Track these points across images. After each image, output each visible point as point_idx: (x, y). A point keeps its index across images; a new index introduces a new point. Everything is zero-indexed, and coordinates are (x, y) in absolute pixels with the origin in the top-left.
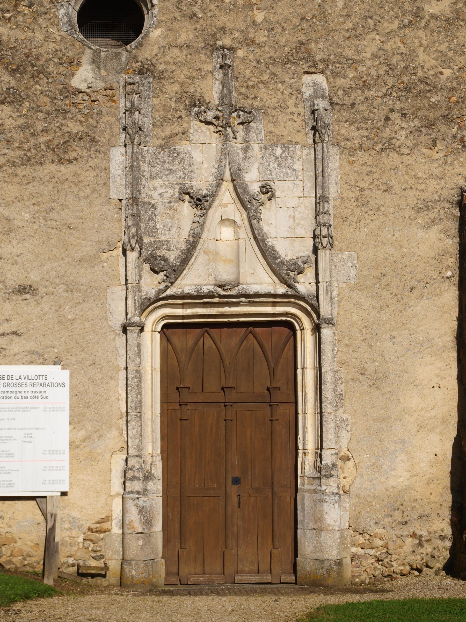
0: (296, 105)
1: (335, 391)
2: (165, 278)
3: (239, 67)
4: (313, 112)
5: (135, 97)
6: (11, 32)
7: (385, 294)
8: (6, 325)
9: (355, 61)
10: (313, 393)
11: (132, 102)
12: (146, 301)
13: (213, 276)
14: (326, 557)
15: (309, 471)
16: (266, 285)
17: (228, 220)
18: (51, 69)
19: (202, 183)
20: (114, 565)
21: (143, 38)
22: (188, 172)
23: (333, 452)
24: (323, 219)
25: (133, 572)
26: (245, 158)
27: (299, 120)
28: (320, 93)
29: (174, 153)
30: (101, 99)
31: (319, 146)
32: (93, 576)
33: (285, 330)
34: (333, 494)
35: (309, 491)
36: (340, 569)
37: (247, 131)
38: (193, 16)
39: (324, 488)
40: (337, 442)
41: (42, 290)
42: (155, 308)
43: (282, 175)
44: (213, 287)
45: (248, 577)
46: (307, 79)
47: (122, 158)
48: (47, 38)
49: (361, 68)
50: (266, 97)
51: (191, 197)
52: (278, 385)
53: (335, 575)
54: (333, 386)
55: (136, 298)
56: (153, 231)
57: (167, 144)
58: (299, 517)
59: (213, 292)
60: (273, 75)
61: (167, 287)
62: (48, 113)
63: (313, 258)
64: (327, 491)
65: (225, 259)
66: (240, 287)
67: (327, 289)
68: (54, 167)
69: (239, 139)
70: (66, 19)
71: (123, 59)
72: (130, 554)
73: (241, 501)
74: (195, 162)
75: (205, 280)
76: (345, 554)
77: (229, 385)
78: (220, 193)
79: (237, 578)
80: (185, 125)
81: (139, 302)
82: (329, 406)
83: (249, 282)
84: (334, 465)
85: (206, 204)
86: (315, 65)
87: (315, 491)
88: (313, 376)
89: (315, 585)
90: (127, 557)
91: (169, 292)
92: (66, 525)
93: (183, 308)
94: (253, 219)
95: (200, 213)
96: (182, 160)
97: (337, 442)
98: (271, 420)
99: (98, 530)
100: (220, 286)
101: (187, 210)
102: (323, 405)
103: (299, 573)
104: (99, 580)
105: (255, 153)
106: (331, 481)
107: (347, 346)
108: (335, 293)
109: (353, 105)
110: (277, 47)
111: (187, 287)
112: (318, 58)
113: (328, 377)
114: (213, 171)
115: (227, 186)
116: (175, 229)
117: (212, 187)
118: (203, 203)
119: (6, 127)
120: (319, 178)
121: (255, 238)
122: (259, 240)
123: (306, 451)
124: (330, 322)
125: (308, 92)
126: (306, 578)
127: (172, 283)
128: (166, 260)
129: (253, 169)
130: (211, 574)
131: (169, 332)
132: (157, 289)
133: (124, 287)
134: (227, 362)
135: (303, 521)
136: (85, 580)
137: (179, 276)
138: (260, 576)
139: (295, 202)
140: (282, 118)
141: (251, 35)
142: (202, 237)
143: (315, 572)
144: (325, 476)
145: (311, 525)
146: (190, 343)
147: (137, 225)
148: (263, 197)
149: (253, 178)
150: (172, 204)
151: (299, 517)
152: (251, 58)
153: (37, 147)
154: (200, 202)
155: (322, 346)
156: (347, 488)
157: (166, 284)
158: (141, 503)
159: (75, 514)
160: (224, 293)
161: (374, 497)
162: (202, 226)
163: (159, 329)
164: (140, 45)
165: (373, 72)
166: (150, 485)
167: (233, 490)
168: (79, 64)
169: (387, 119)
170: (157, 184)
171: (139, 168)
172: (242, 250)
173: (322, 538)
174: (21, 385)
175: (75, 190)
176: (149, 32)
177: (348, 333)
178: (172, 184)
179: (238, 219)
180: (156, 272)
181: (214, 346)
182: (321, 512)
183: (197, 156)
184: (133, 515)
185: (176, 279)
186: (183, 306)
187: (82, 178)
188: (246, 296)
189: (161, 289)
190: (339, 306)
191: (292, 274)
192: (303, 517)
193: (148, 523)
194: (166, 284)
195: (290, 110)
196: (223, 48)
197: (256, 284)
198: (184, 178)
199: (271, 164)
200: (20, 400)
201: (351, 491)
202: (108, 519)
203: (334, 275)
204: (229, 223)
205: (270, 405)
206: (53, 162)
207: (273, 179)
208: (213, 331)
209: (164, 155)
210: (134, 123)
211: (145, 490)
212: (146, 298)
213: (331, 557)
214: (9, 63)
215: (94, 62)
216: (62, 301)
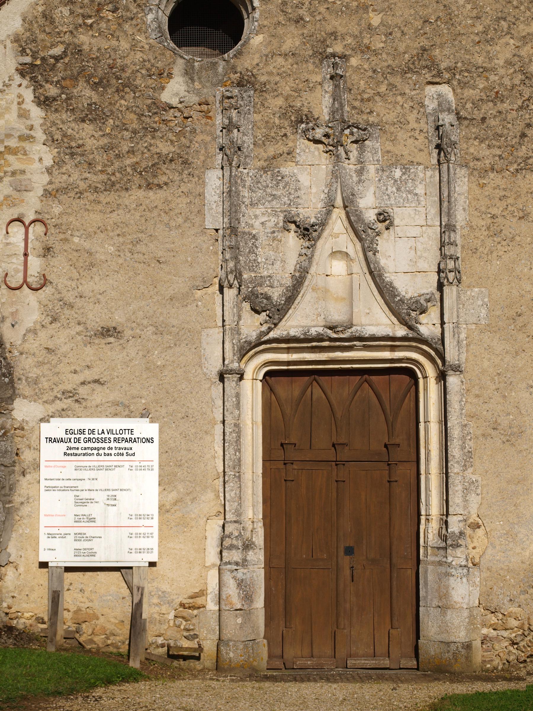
0: (418, 120)
1: (463, 448)
2: (268, 318)
3: (353, 78)
4: (437, 128)
5: (234, 113)
6: (93, 41)
7: (521, 336)
8: (87, 372)
9: (485, 70)
10: (438, 451)
11: (230, 119)
12: (246, 345)
13: (323, 317)
14: (452, 639)
15: (433, 540)
16: (383, 327)
17: (340, 252)
18: (138, 82)
19: (309, 210)
20: (209, 646)
21: (243, 45)
22: (294, 198)
23: (461, 518)
24: (449, 250)
25: (231, 654)
26: (360, 181)
27: (421, 138)
28: (445, 106)
29: (277, 176)
30: (195, 115)
31: (445, 167)
32: (185, 658)
33: (406, 379)
34: (461, 566)
35: (433, 563)
36: (468, 653)
37: (362, 151)
38: (299, 20)
39: (450, 559)
40: (465, 507)
41: (128, 333)
43: (402, 201)
44: (322, 328)
45: (363, 662)
46: (431, 90)
47: (219, 183)
48: (133, 47)
49: (492, 78)
50: (383, 112)
51: (298, 226)
52: (397, 441)
53: (463, 660)
54: (460, 443)
55: (234, 341)
56: (254, 266)
57: (270, 166)
58: (422, 593)
59: (322, 335)
60: (392, 86)
61: (270, 329)
62: (135, 132)
63: (437, 295)
64: (454, 563)
65: (336, 296)
66: (354, 329)
67: (454, 332)
68: (141, 193)
69: (353, 160)
70: (155, 25)
71: (220, 69)
72: (228, 634)
73: (355, 574)
74: (302, 186)
75: (313, 320)
76: (474, 636)
77: (341, 441)
78: (330, 222)
79: (350, 662)
80: (291, 144)
81: (237, 346)
82: (456, 465)
83: (363, 323)
84: (461, 533)
85: (315, 234)
86: (439, 74)
87: (440, 563)
88: (438, 430)
89: (440, 671)
90: (224, 638)
91: (272, 335)
92: (155, 600)
93: (288, 353)
94: (369, 251)
95: (307, 244)
96: (287, 184)
97: (465, 507)
98: (389, 482)
99: (191, 605)
100: (330, 328)
101: (292, 241)
102: (449, 464)
103: (421, 657)
104: (192, 663)
105: (370, 175)
106: (459, 552)
107: (477, 396)
108: (463, 336)
109: (484, 119)
110: (396, 54)
111: (292, 329)
112: (443, 66)
113: (455, 432)
114: (323, 196)
115: (338, 214)
116: (279, 262)
117: (321, 215)
118: (311, 233)
119: (87, 148)
120: (445, 203)
121: (371, 273)
122: (375, 274)
123: (430, 518)
124: (457, 369)
125: (431, 105)
126: (429, 663)
127: (276, 325)
128: (268, 298)
129: (368, 194)
130: (320, 657)
131: (272, 380)
132: (258, 332)
133: (221, 330)
134: (339, 415)
135: (425, 598)
136: (176, 663)
137: (284, 317)
138: (376, 660)
139: (415, 231)
140: (401, 135)
141: (366, 41)
142: (309, 272)
143: (440, 657)
144: (451, 545)
145: (435, 603)
146: (297, 393)
147: (236, 258)
148: (380, 226)
149: (368, 204)
150: (275, 235)
151: (421, 592)
152: (366, 66)
153: (122, 170)
154: (308, 232)
155: (448, 397)
156: (477, 560)
157: (268, 325)
158: (240, 575)
159: (165, 587)
160: (335, 336)
161: (508, 571)
162: (310, 259)
163: (261, 377)
164: (239, 53)
165: (507, 82)
166: (251, 555)
167: (346, 561)
168: (170, 76)
169: (523, 135)
170: (258, 212)
171: (238, 193)
172: (356, 286)
173: (448, 617)
174: (104, 440)
175: (165, 218)
176: (249, 39)
177: (477, 381)
178: (276, 211)
179: (351, 251)
180: (258, 312)
181: (324, 396)
182: (447, 587)
183: (304, 179)
184: (231, 589)
185: (281, 320)
186: (288, 350)
187: (173, 205)
188: (361, 339)
189: (263, 332)
190: (467, 351)
191: (413, 314)
192: (426, 592)
193: (248, 598)
194: (268, 325)
195: (411, 126)
196: (334, 55)
197: (372, 325)
198: (290, 204)
199: (389, 188)
200: (102, 458)
201: (482, 563)
202: (202, 593)
203: (462, 315)
204: (340, 255)
205: (388, 465)
206: (140, 187)
207: (391, 205)
208: (323, 380)
209: (266, 179)
210: (232, 142)
211: (245, 560)
213: (458, 640)
214: (91, 76)
215: (186, 73)
216: (150, 345)
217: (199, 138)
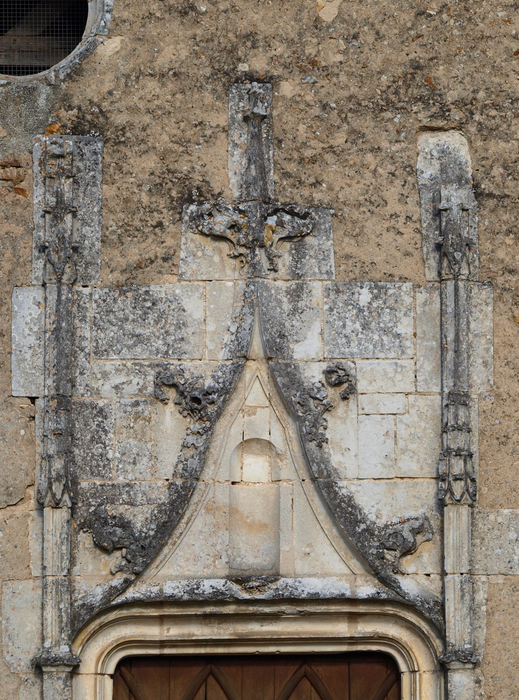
2: (124, 563)
12: (83, 612)
13: (225, 559)
42: (102, 627)
44: (223, 581)
55: (62, 606)
59: (223, 594)
61: (128, 583)
75: (207, 566)
91: (131, 594)
127: (138, 575)
132: (107, 587)
133: (39, 583)
157: (125, 576)
186: (161, 620)
189: (115, 587)
194: (125, 576)
212: (83, 605)
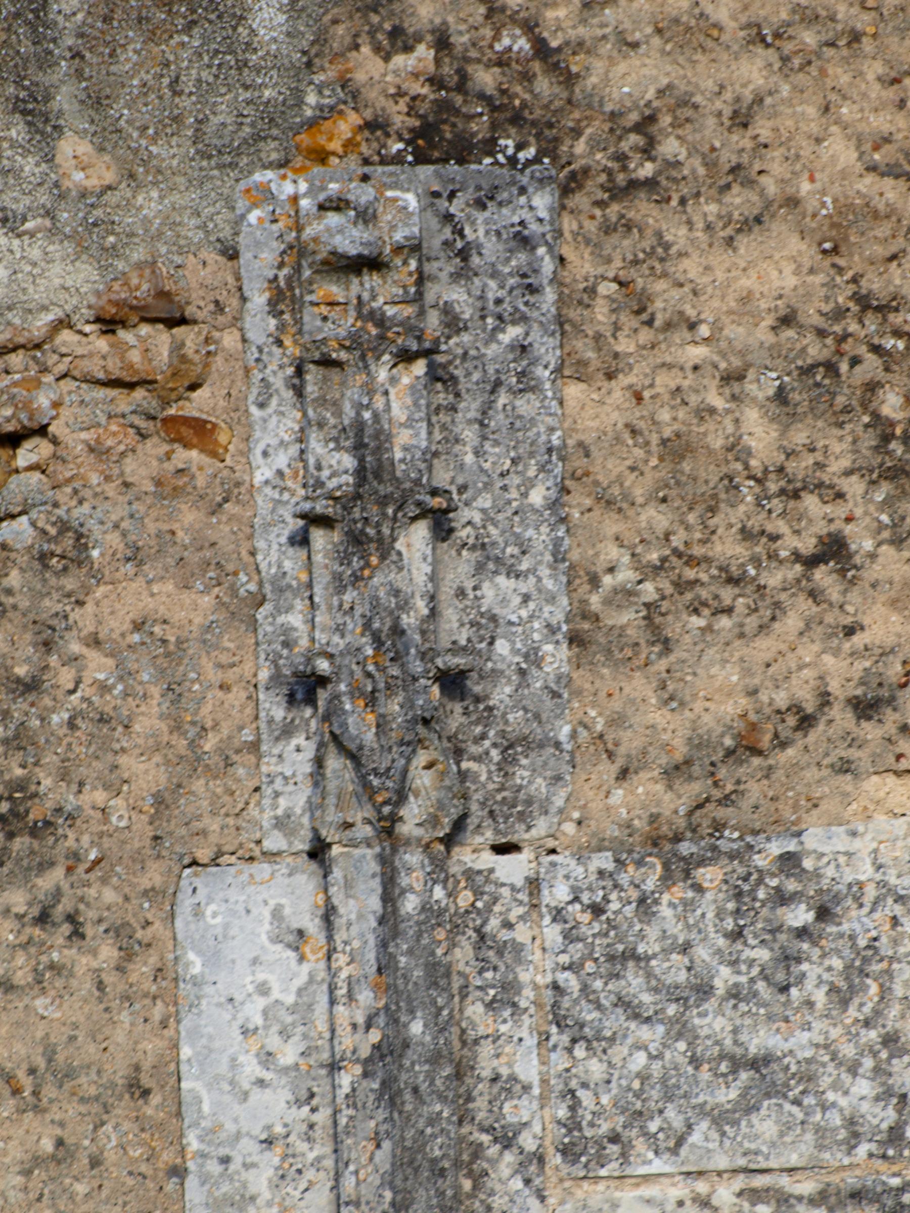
5: (397, 394)
11: (367, 442)
29: (782, 898)
30: (77, 417)
47: (290, 976)
209: (687, 924)
210: (389, 639)
217: (115, 605)
